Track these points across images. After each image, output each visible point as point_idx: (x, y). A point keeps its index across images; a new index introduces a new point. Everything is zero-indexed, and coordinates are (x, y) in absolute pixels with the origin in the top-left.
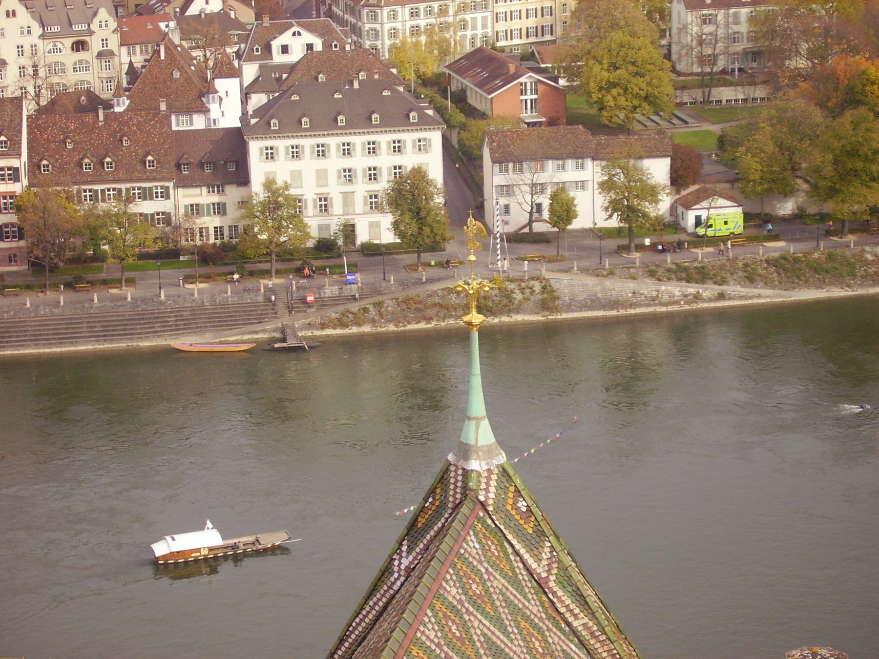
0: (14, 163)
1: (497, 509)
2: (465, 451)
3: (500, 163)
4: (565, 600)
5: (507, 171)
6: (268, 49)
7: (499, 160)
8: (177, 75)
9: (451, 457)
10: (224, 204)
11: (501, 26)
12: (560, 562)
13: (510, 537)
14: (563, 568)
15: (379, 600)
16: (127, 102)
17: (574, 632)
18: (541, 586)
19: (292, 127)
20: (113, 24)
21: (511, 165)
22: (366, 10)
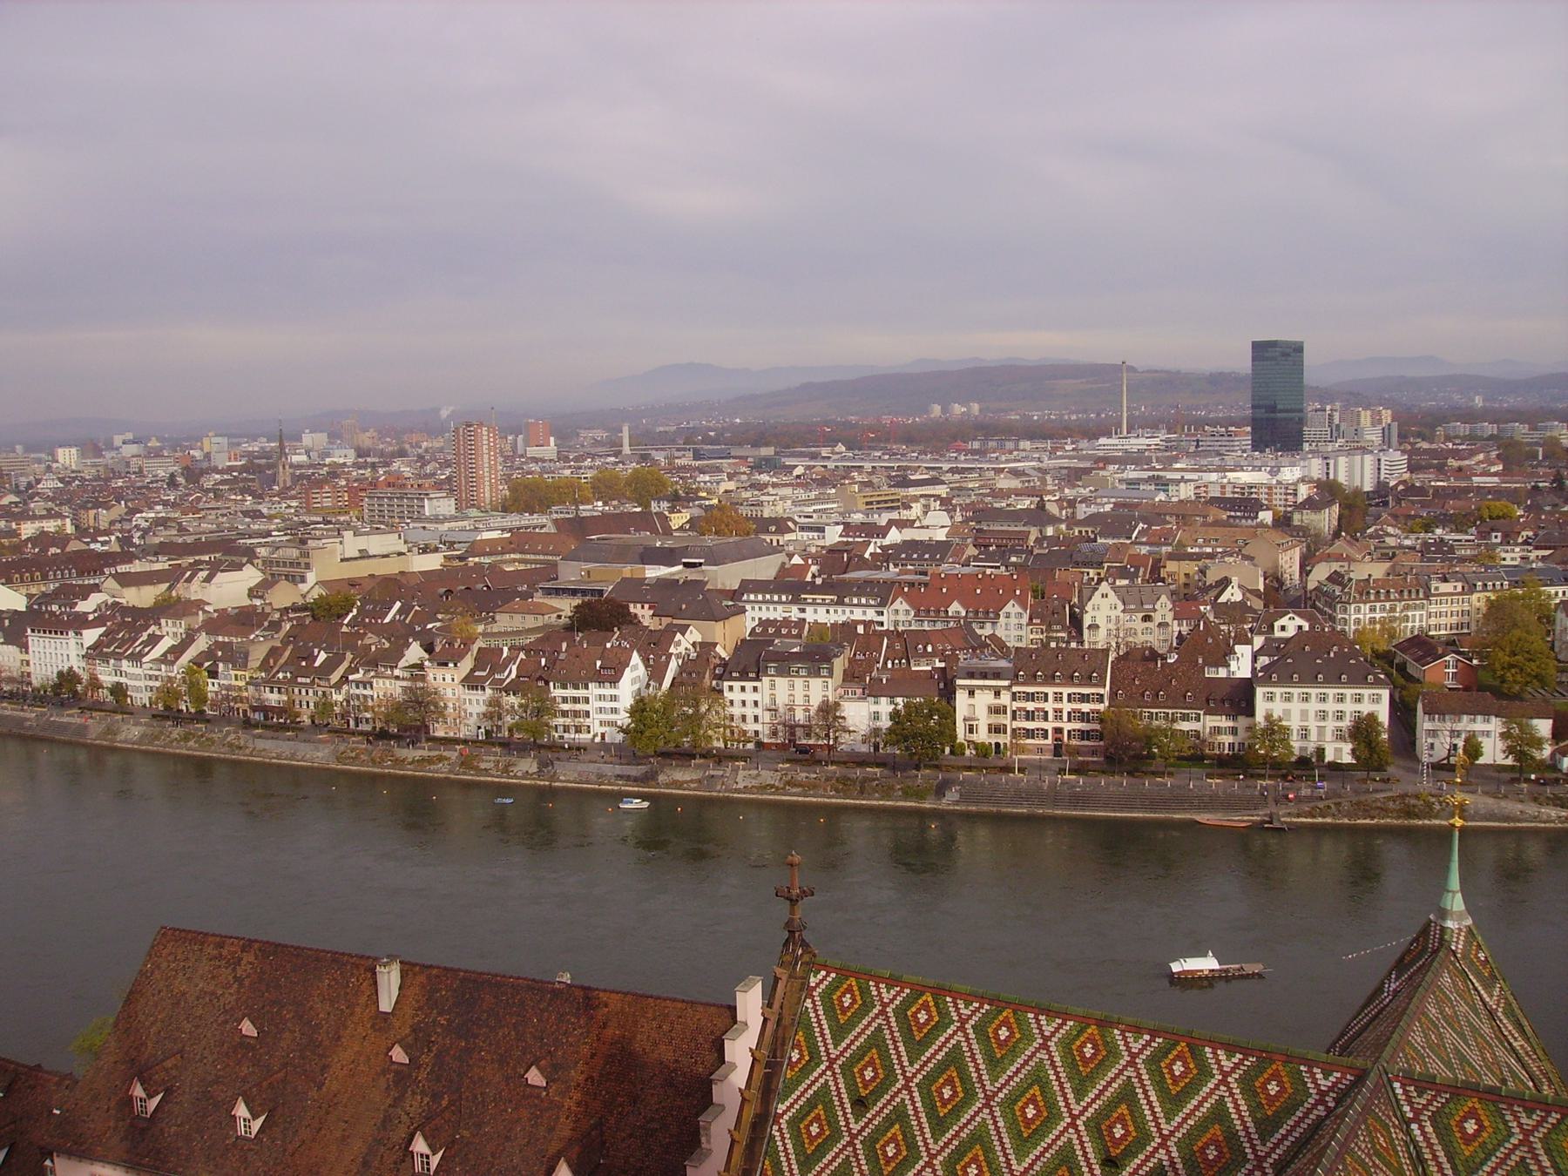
0: (1101, 691)
1: (1464, 957)
2: (1443, 914)
3: (1430, 714)
4: (1508, 1026)
6: (1272, 627)
7: (1429, 712)
8: (1210, 641)
9: (1432, 917)
11: (1433, 621)
12: (1506, 999)
13: (1471, 977)
14: (1508, 1004)
15: (1372, 1010)
16: (1176, 657)
17: (1513, 1049)
18: (1492, 1014)
19: (1286, 680)
22: (1339, 605)
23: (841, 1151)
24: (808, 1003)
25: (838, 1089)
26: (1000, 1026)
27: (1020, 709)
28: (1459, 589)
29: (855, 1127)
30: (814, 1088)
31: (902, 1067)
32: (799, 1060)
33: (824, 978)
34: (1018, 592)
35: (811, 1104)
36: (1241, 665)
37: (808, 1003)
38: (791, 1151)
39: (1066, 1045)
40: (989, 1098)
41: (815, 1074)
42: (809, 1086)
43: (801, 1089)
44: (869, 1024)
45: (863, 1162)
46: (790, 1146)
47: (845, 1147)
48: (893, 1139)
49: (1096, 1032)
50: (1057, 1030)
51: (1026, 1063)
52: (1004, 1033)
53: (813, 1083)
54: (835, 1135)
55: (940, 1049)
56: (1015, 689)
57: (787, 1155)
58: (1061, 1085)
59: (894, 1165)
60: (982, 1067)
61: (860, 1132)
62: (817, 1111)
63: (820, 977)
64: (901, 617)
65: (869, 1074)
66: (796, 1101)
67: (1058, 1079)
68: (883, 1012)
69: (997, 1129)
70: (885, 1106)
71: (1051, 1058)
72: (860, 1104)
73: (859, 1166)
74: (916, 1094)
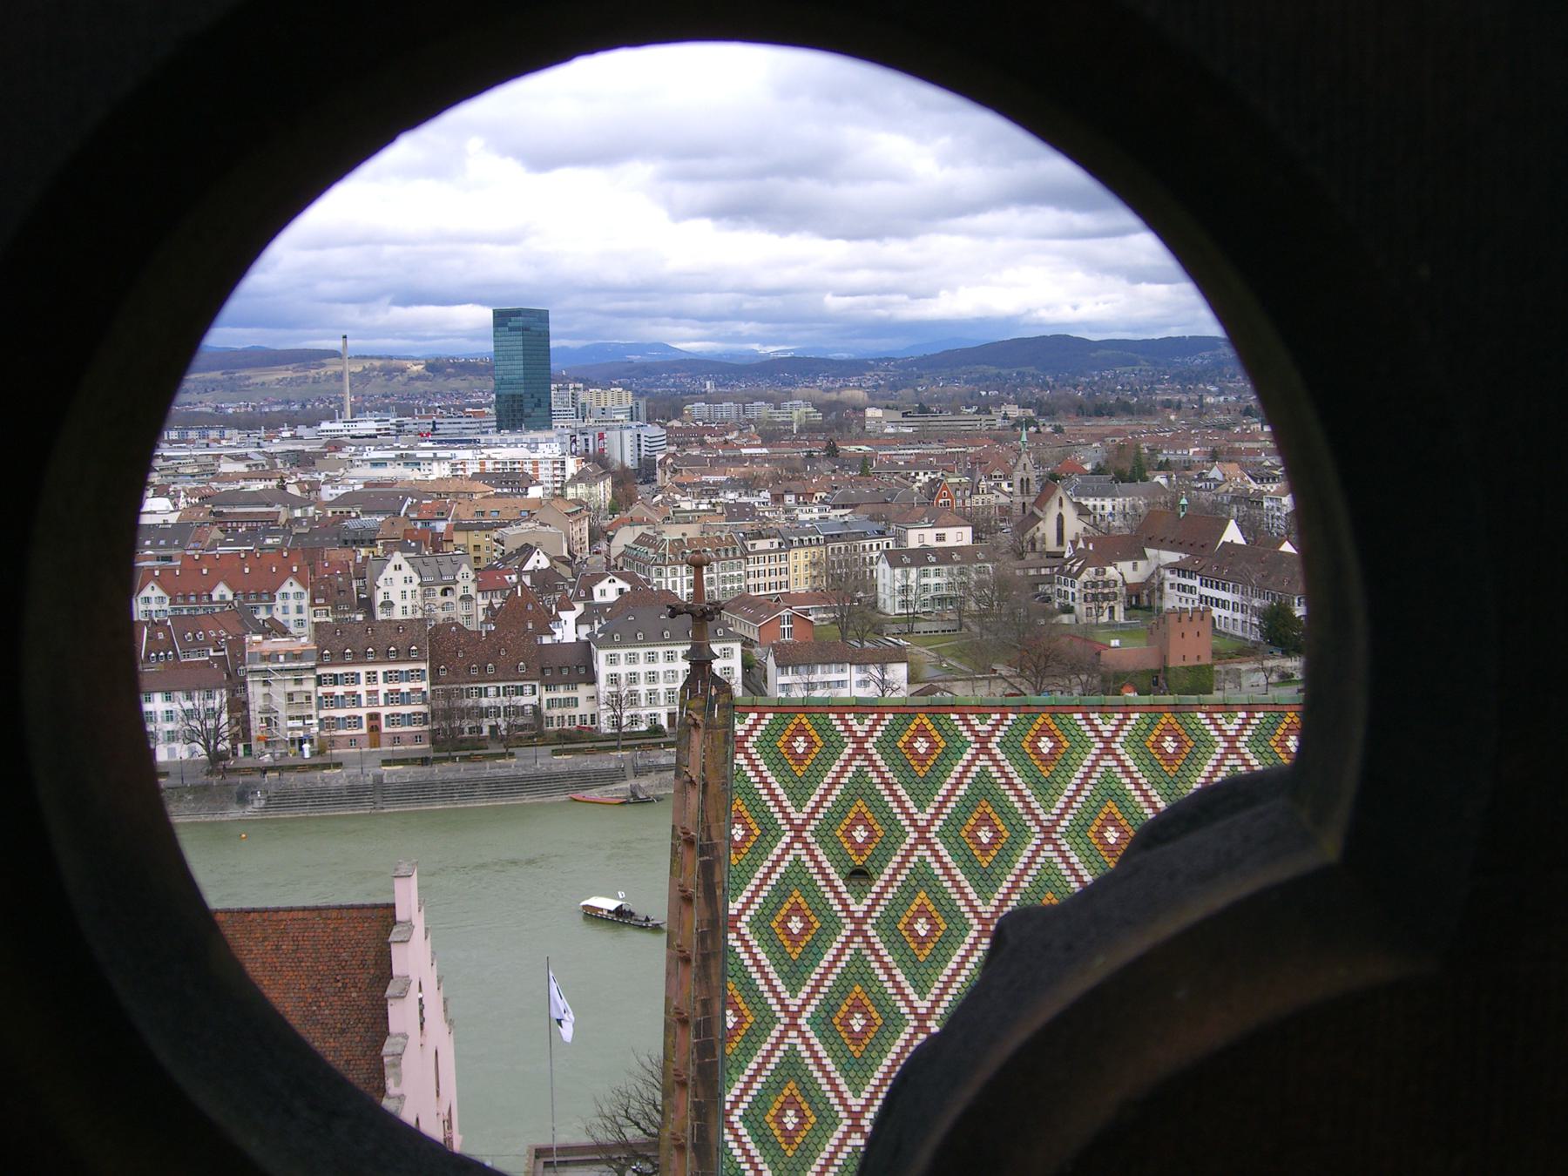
3: (782, 667)
5: (787, 673)
6: (590, 594)
7: (782, 665)
8: (530, 607)
10: (577, 699)
11: (751, 581)
19: (629, 640)
20: (472, 576)
21: (790, 669)
23: (846, 945)
24: (740, 759)
25: (818, 864)
26: (1038, 737)
27: (326, 695)
28: (776, 545)
29: (859, 909)
30: (780, 870)
31: (910, 817)
32: (746, 837)
33: (756, 723)
34: (295, 569)
35: (782, 892)
36: (567, 630)
37: (740, 759)
38: (766, 962)
39: (1137, 743)
40: (1048, 832)
41: (777, 851)
42: (772, 870)
43: (759, 875)
44: (843, 770)
45: (884, 952)
46: (761, 956)
47: (849, 940)
48: (922, 911)
49: (1172, 721)
50: (1119, 727)
51: (1087, 776)
52: (1045, 745)
53: (776, 863)
54: (831, 925)
55: (959, 781)
56: (320, 671)
57: (760, 968)
58: (1145, 794)
59: (931, 945)
60: (1027, 792)
61: (868, 914)
62: (792, 900)
63: (749, 721)
64: (154, 606)
65: (860, 834)
66: (755, 893)
67: (1138, 786)
68: (860, 750)
69: (1071, 867)
70: (896, 872)
71: (1121, 763)
72: (859, 876)
73: (879, 959)
74: (939, 847)
